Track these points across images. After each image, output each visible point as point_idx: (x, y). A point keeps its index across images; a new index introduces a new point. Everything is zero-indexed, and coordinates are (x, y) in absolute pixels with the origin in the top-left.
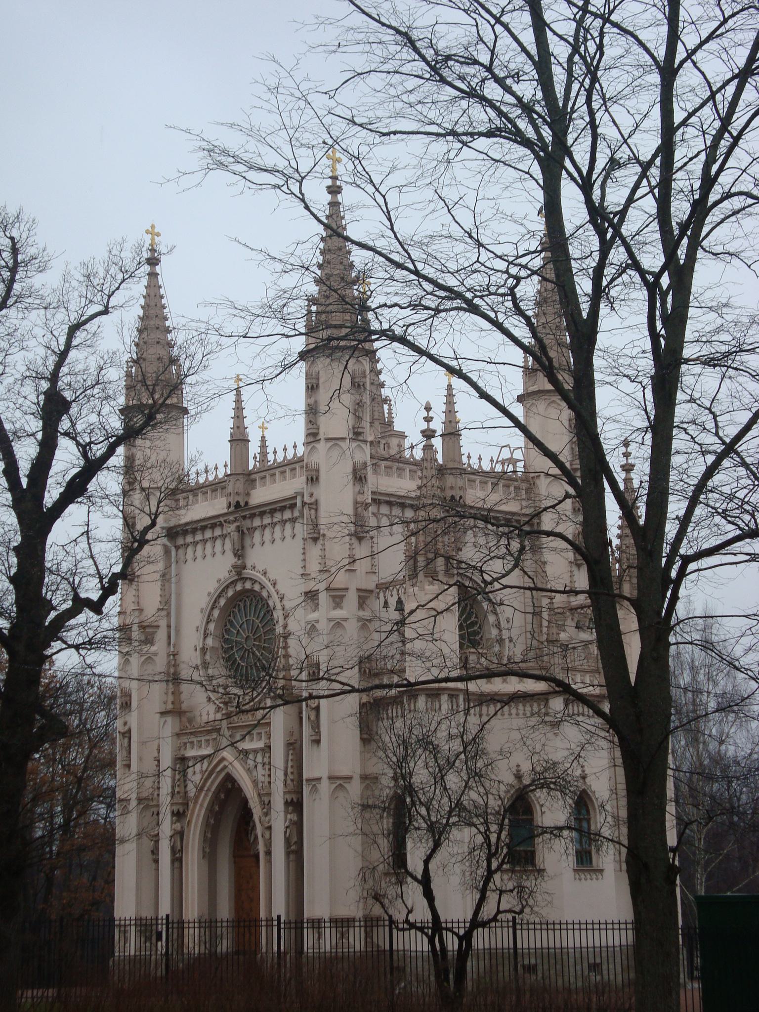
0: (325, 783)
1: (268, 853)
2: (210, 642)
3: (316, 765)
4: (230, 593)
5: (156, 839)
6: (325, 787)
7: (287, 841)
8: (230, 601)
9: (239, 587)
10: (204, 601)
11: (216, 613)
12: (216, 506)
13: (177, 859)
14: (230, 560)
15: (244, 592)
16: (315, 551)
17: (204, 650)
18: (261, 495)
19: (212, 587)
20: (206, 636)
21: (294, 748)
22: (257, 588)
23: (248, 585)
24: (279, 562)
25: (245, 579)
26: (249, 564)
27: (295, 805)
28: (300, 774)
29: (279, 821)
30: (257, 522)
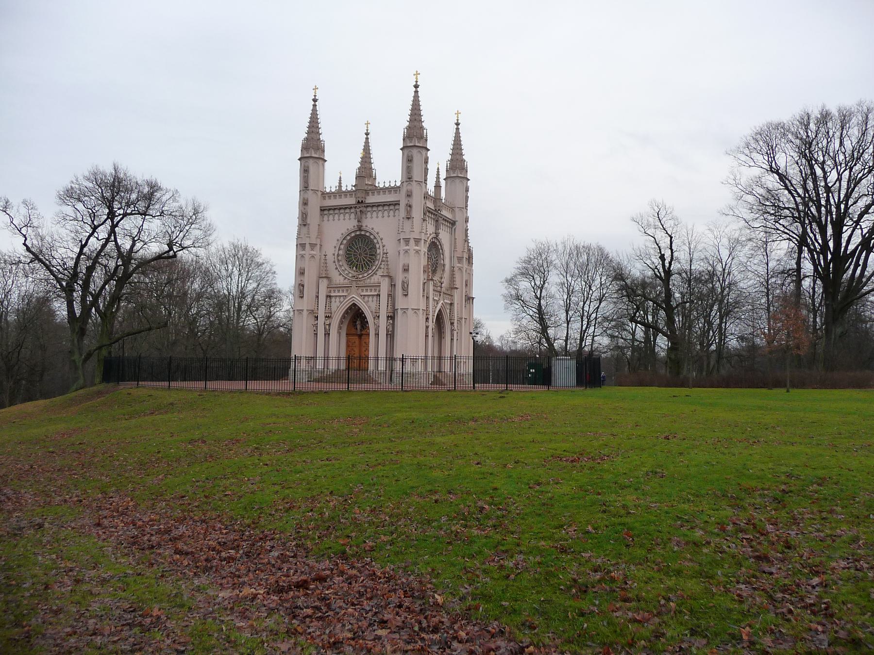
0: (410, 310)
1: (377, 335)
2: (341, 252)
3: (401, 303)
4: (353, 235)
5: (316, 326)
6: (410, 312)
7: (387, 331)
8: (352, 238)
9: (358, 233)
10: (339, 236)
11: (345, 242)
12: (351, 201)
13: (327, 334)
14: (355, 223)
15: (361, 235)
16: (407, 223)
17: (338, 255)
18: (371, 199)
19: (344, 231)
20: (339, 249)
21: (391, 296)
22: (368, 234)
23: (363, 233)
24: (379, 226)
25: (360, 230)
26: (364, 225)
27: (392, 317)
28: (394, 305)
29: (383, 322)
30: (369, 209)
